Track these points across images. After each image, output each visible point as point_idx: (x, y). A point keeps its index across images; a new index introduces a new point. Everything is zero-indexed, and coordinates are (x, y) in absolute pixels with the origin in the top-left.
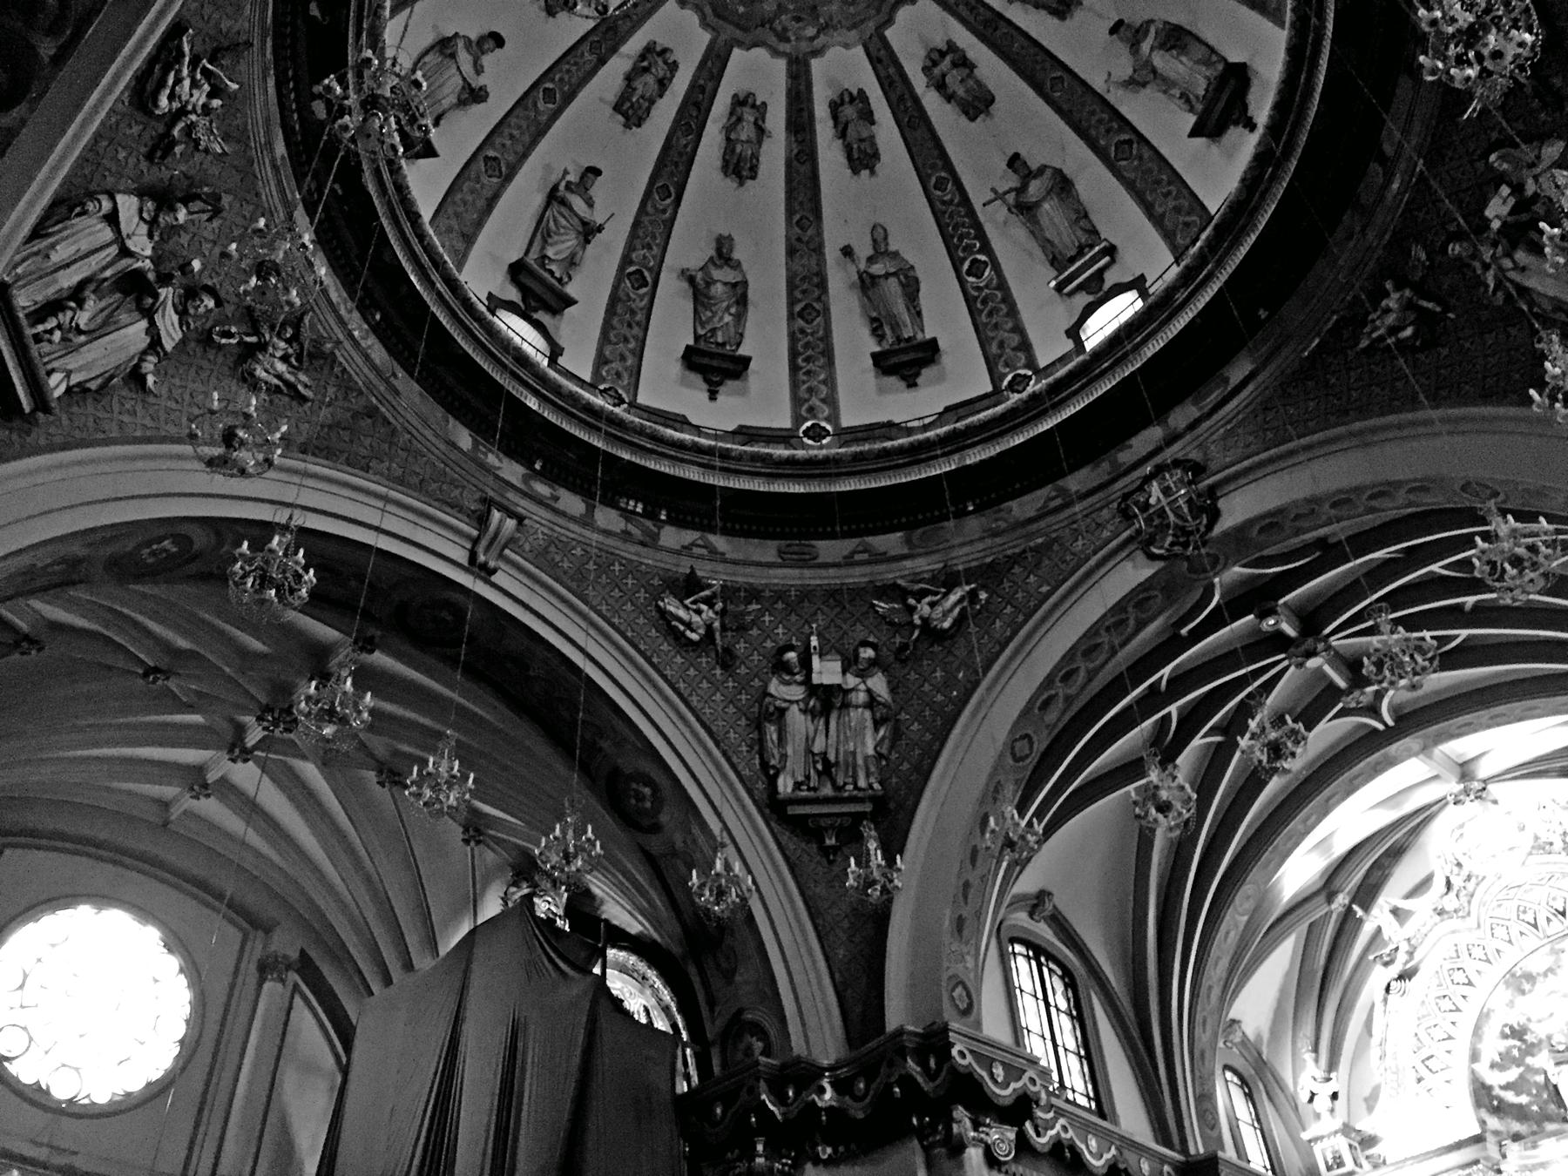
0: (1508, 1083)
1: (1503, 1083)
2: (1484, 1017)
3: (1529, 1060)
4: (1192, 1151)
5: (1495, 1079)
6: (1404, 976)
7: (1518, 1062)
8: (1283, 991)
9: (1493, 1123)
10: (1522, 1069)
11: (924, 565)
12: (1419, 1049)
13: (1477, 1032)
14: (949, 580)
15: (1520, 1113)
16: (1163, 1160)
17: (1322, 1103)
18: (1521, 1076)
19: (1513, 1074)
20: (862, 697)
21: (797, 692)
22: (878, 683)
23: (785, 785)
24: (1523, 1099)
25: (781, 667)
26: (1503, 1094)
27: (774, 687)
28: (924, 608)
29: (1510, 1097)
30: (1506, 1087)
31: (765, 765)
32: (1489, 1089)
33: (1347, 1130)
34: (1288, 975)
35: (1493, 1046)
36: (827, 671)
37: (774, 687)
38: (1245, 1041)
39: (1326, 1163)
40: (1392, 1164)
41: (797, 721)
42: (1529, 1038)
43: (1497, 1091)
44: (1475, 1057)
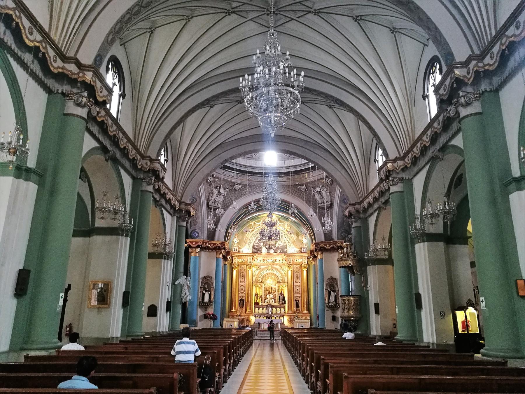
5: (255, 245)
6: (252, 231)
9: (253, 250)
11: (239, 181)
13: (256, 239)
14: (240, 184)
15: (256, 249)
19: (257, 245)
20: (223, 194)
21: (217, 192)
22: (226, 193)
23: (210, 203)
25: (216, 187)
27: (214, 190)
28: (235, 186)
29: (256, 247)
31: (208, 199)
36: (222, 191)
37: (214, 190)
40: (225, 240)
41: (215, 195)
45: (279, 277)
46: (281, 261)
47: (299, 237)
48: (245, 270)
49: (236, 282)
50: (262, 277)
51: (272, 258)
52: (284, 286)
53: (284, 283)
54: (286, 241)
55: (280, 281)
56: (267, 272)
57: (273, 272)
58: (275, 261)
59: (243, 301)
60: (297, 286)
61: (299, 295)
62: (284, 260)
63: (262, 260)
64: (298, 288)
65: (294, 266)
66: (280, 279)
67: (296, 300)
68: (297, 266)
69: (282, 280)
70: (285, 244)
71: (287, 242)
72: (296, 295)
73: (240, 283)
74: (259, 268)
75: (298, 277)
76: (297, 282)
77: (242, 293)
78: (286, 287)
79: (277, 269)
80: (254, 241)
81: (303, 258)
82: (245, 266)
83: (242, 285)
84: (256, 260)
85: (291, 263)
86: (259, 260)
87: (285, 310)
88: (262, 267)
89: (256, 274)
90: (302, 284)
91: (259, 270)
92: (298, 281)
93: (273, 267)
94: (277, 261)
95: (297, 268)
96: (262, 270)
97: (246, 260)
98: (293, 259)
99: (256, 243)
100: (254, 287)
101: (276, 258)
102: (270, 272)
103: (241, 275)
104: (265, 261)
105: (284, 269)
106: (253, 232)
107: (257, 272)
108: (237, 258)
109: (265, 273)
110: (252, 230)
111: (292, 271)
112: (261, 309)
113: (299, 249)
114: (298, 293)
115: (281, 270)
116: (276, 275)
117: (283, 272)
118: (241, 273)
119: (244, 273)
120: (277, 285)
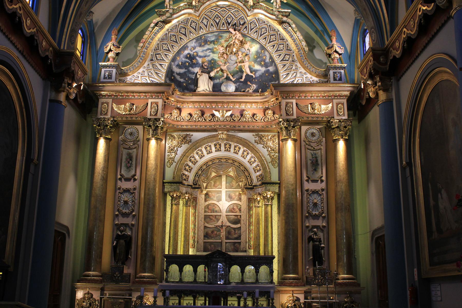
0: (180, 73)
1: (178, 72)
2: (185, 48)
3: (190, 68)
4: (62, 47)
5: (176, 70)
7: (186, 68)
8: (114, 10)
10: (187, 70)
12: (157, 49)
13: (179, 53)
16: (51, 45)
17: (111, 55)
18: (185, 72)
19: (182, 71)
24: (182, 80)
26: (176, 76)
29: (178, 78)
30: (179, 74)
32: (173, 72)
33: (117, 67)
34: (119, 5)
35: (181, 59)
38: (90, 23)
39: (105, 75)
42: (194, 61)
43: (175, 74)
44: (174, 60)
45: (251, 168)
46: (260, 116)
47: (315, 51)
48: (136, 141)
49: (105, 179)
50: (195, 168)
51: (231, 106)
52: (269, 194)
53: (269, 187)
54: (275, 56)
55: (255, 182)
56: (215, 154)
57: (231, 154)
58: (237, 114)
59: (128, 240)
60: (315, 192)
61: (320, 223)
62: (270, 112)
63: (196, 114)
64: (316, 199)
65: (304, 128)
66: (255, 176)
67: (310, 239)
68: (314, 129)
69: (261, 177)
70: (271, 69)
71: (277, 61)
72: (310, 223)
73: (119, 184)
74: (185, 140)
75: (315, 164)
76: (314, 181)
77: (125, 215)
78: (275, 202)
79: (245, 143)
80: (171, 56)
81: (335, 101)
82: (140, 128)
83: (127, 191)
84: (175, 112)
85: (295, 117)
86: (185, 114)
87: (272, 272)
88: (197, 136)
89: (177, 158)
90: (332, 186)
91: (185, 147)
92: (319, 174)
93: (234, 137)
94: (248, 114)
95: (313, 135)
96: (196, 145)
97: (141, 106)
98: (302, 104)
99: (178, 66)
100: (169, 198)
101: (243, 106)
102: (223, 153)
103: (124, 157)
104: (207, 115)
105: (270, 144)
106: (167, 26)
107: (180, 151)
108: (110, 101)
109: (207, 157)
110: (164, 18)
111: (298, 142)
112: (188, 268)
113: (317, 76)
114: (316, 217)
115: (260, 147)
116: (241, 164)
117: (264, 152)
118: (125, 152)
119: (134, 152)
120: (244, 198)
